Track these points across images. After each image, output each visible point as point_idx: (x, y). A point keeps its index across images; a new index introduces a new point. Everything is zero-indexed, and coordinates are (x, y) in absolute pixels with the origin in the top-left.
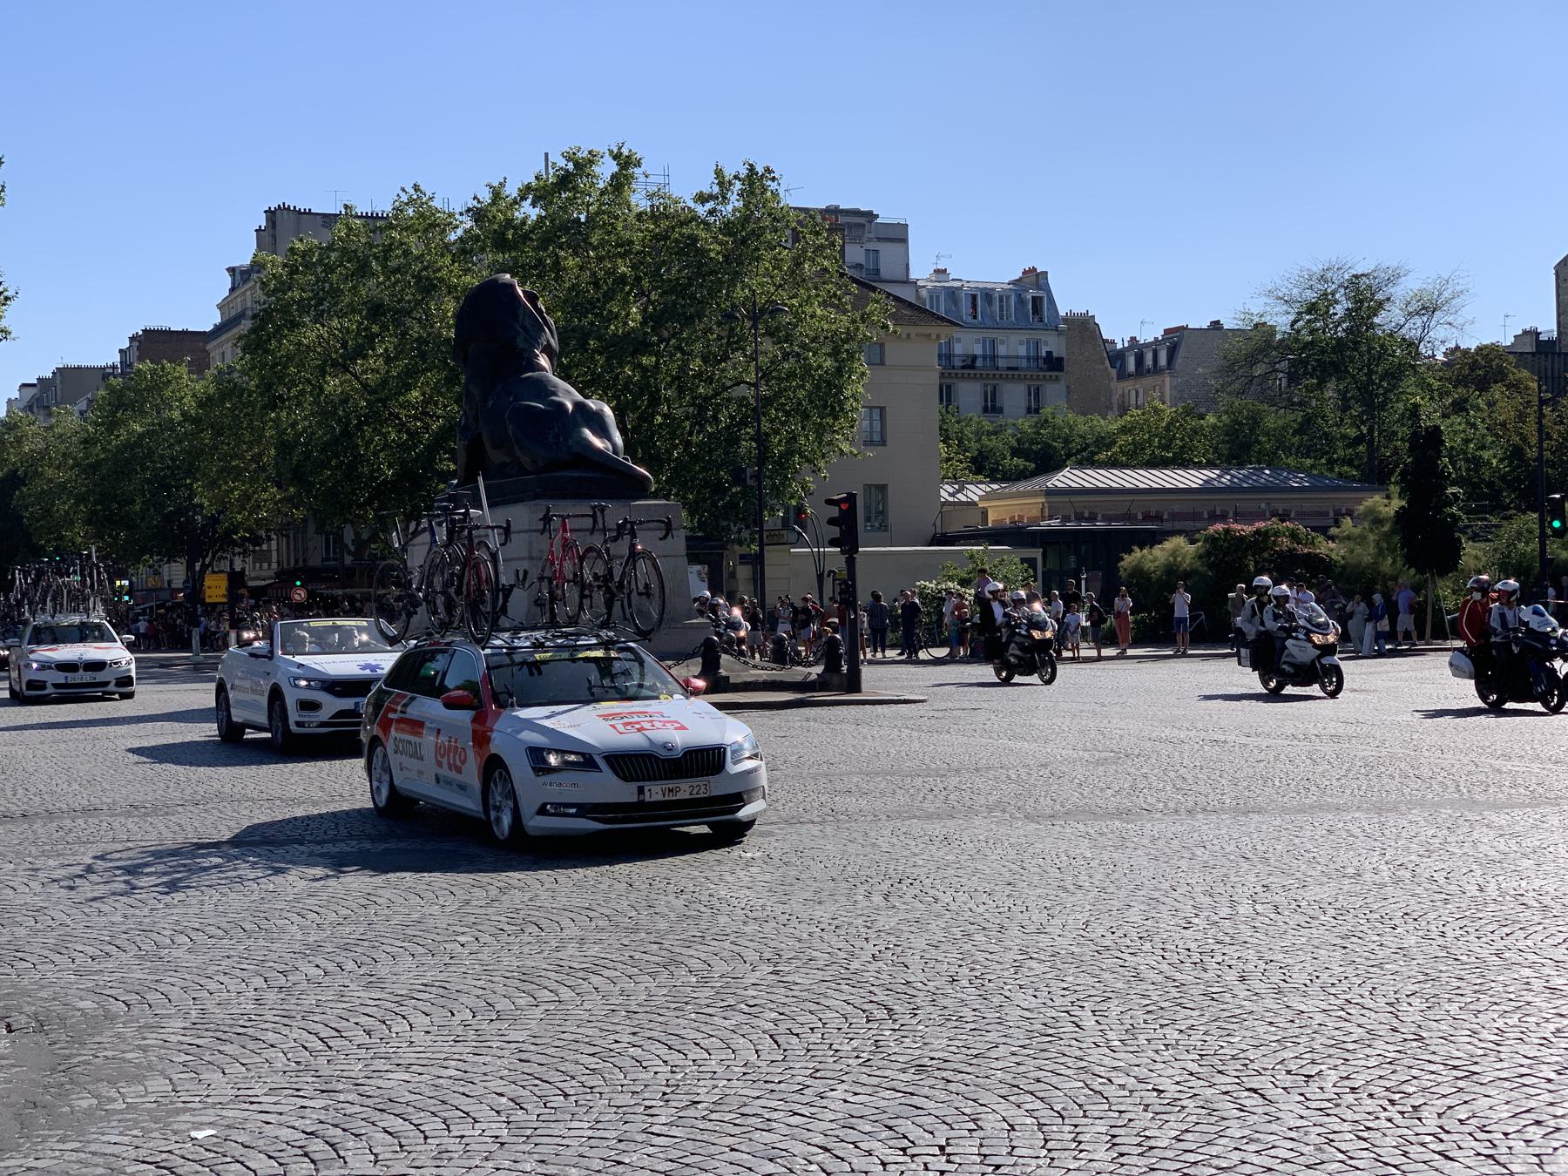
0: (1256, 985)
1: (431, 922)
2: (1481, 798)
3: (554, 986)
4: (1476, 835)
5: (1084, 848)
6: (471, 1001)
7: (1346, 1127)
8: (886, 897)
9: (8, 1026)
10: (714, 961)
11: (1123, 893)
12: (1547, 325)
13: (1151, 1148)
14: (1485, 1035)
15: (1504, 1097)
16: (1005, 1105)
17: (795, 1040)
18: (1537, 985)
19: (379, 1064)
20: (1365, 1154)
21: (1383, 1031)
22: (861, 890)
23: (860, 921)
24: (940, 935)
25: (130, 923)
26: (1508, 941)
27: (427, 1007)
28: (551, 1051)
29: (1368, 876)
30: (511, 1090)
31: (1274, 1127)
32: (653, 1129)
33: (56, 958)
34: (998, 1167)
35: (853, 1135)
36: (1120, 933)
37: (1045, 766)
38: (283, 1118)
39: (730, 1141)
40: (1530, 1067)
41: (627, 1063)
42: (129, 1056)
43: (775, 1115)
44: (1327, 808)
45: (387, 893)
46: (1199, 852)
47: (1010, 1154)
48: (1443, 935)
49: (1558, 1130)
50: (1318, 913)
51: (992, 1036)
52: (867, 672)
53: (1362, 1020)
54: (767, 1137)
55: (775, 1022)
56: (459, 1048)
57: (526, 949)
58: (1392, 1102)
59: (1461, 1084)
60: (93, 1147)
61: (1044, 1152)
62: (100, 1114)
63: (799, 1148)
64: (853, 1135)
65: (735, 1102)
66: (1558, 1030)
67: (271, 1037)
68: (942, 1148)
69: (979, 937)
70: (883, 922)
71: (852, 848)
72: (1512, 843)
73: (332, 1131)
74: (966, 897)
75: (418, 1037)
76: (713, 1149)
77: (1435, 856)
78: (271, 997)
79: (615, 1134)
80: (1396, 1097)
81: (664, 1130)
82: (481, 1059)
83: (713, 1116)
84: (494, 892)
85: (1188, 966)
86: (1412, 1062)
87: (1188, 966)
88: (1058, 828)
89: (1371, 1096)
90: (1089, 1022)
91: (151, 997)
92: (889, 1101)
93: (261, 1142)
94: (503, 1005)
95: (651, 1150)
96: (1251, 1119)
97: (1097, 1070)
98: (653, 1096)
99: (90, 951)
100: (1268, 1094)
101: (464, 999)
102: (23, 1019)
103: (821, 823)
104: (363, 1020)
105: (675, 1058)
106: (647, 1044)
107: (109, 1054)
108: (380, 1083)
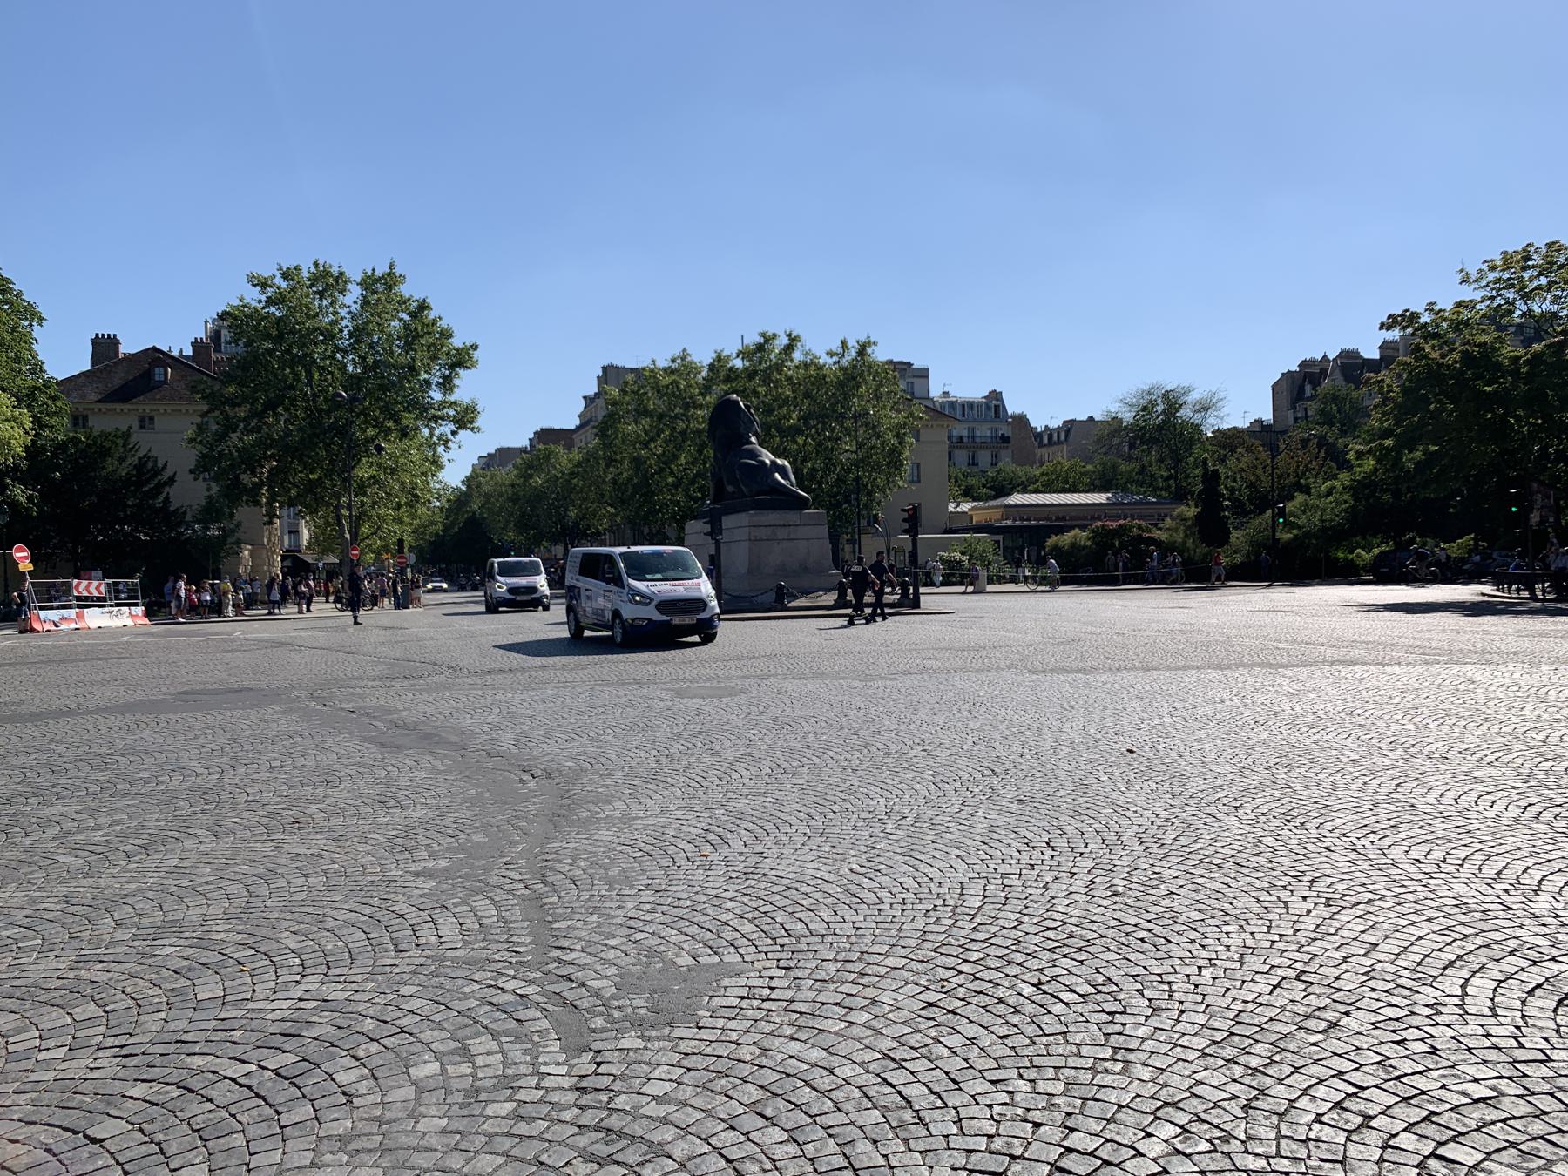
0: (1188, 758)
1: (734, 724)
2: (1273, 662)
3: (809, 756)
4: (1278, 682)
5: (1067, 687)
6: (769, 764)
7: (1266, 834)
8: (970, 711)
9: (532, 775)
10: (889, 744)
11: (1098, 711)
12: (1267, 415)
13: (1163, 845)
14: (1324, 785)
15: (1350, 818)
16: (1073, 821)
17: (947, 786)
18: (1344, 759)
19: (730, 795)
20: (1282, 848)
21: (1268, 782)
22: (955, 707)
23: (960, 724)
24: (1006, 732)
25: (580, 723)
26: (1318, 736)
27: (746, 766)
28: (819, 789)
29: (1228, 703)
30: (807, 810)
31: (1227, 834)
32: (887, 831)
33: (547, 740)
34: (1082, 854)
35: (996, 836)
36: (1103, 732)
37: (1031, 645)
38: (689, 822)
39: (931, 838)
40: (1357, 802)
41: (861, 797)
42: (600, 790)
43: (950, 825)
44: (1193, 668)
45: (707, 708)
46: (1131, 690)
47: (1086, 847)
48: (1281, 733)
49: (1386, 836)
50: (1208, 721)
51: (1054, 785)
52: (922, 598)
53: (1254, 777)
54: (950, 836)
55: (933, 776)
56: (769, 787)
57: (788, 737)
58: (1288, 821)
59: (1322, 811)
60: (596, 837)
61: (1104, 846)
62: (593, 819)
63: (969, 842)
64: (996, 836)
65: (926, 818)
66: (1365, 783)
67: (669, 780)
68: (1047, 843)
69: (1028, 733)
70: (971, 725)
71: (942, 687)
72: (1300, 685)
73: (717, 829)
74: (1012, 713)
75: (747, 781)
76: (923, 842)
77: (1260, 692)
78: (664, 760)
79: (867, 833)
80: (1289, 818)
81: (893, 831)
82: (783, 793)
83: (917, 824)
84: (761, 708)
85: (1147, 749)
86: (1291, 800)
87: (1147, 749)
88: (1049, 678)
89: (1274, 817)
90: (1105, 778)
91: (602, 760)
92: (1012, 819)
93: (682, 835)
94: (785, 765)
95: (889, 842)
96: (1213, 830)
97: (1118, 803)
98: (881, 813)
99: (564, 737)
100: (1217, 816)
101: (764, 762)
102: (540, 772)
103: (922, 673)
104: (715, 772)
105: (885, 793)
106: (868, 787)
107: (589, 789)
108: (734, 804)
